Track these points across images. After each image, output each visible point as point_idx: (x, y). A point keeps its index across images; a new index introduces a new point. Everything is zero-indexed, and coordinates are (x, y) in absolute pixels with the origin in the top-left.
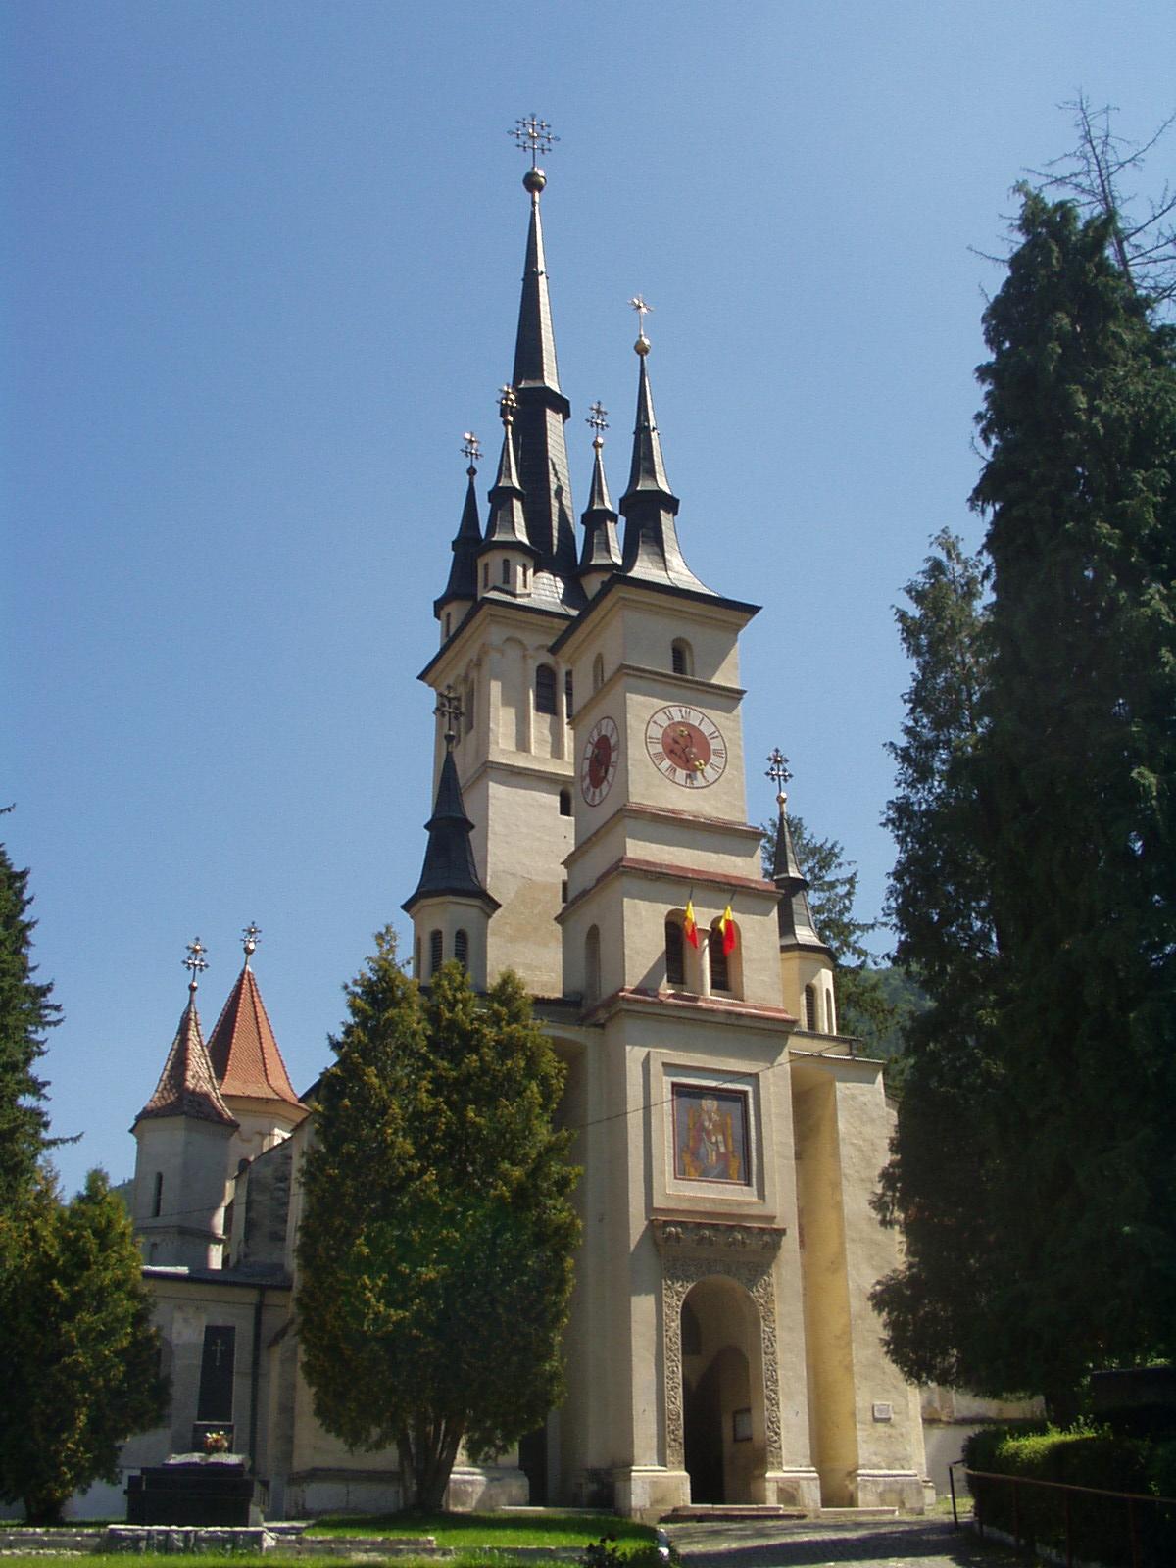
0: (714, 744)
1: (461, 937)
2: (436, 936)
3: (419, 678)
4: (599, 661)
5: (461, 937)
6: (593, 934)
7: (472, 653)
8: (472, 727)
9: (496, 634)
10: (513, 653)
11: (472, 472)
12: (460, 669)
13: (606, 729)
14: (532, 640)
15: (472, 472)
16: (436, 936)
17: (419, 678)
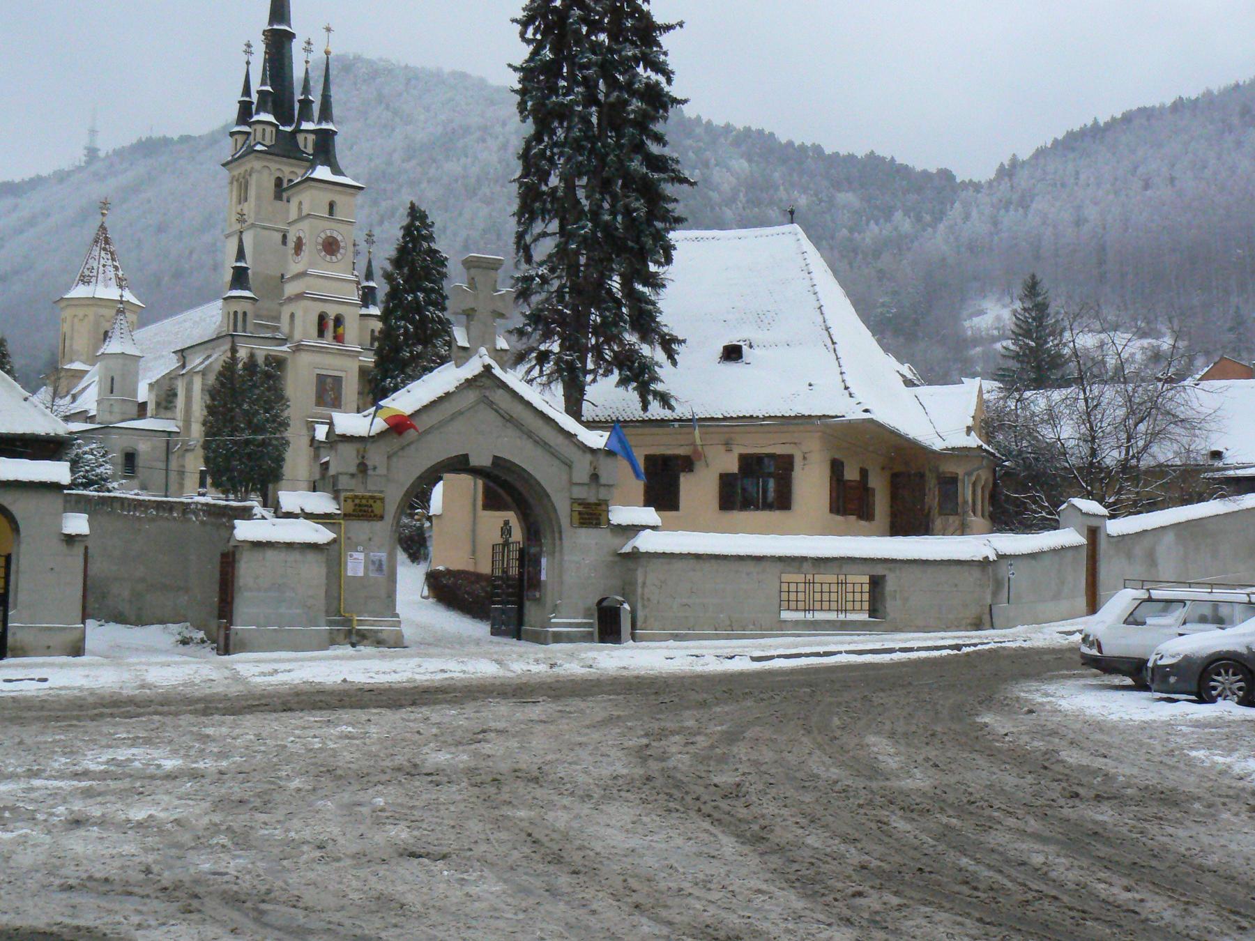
0: (342, 244)
1: (245, 314)
2: (236, 313)
3: (224, 165)
4: (300, 203)
5: (245, 314)
6: (292, 315)
7: (248, 167)
8: (246, 200)
9: (257, 165)
10: (266, 172)
11: (248, 63)
12: (242, 170)
13: (302, 235)
14: (273, 166)
15: (248, 63)
16: (236, 313)
17: (224, 165)
